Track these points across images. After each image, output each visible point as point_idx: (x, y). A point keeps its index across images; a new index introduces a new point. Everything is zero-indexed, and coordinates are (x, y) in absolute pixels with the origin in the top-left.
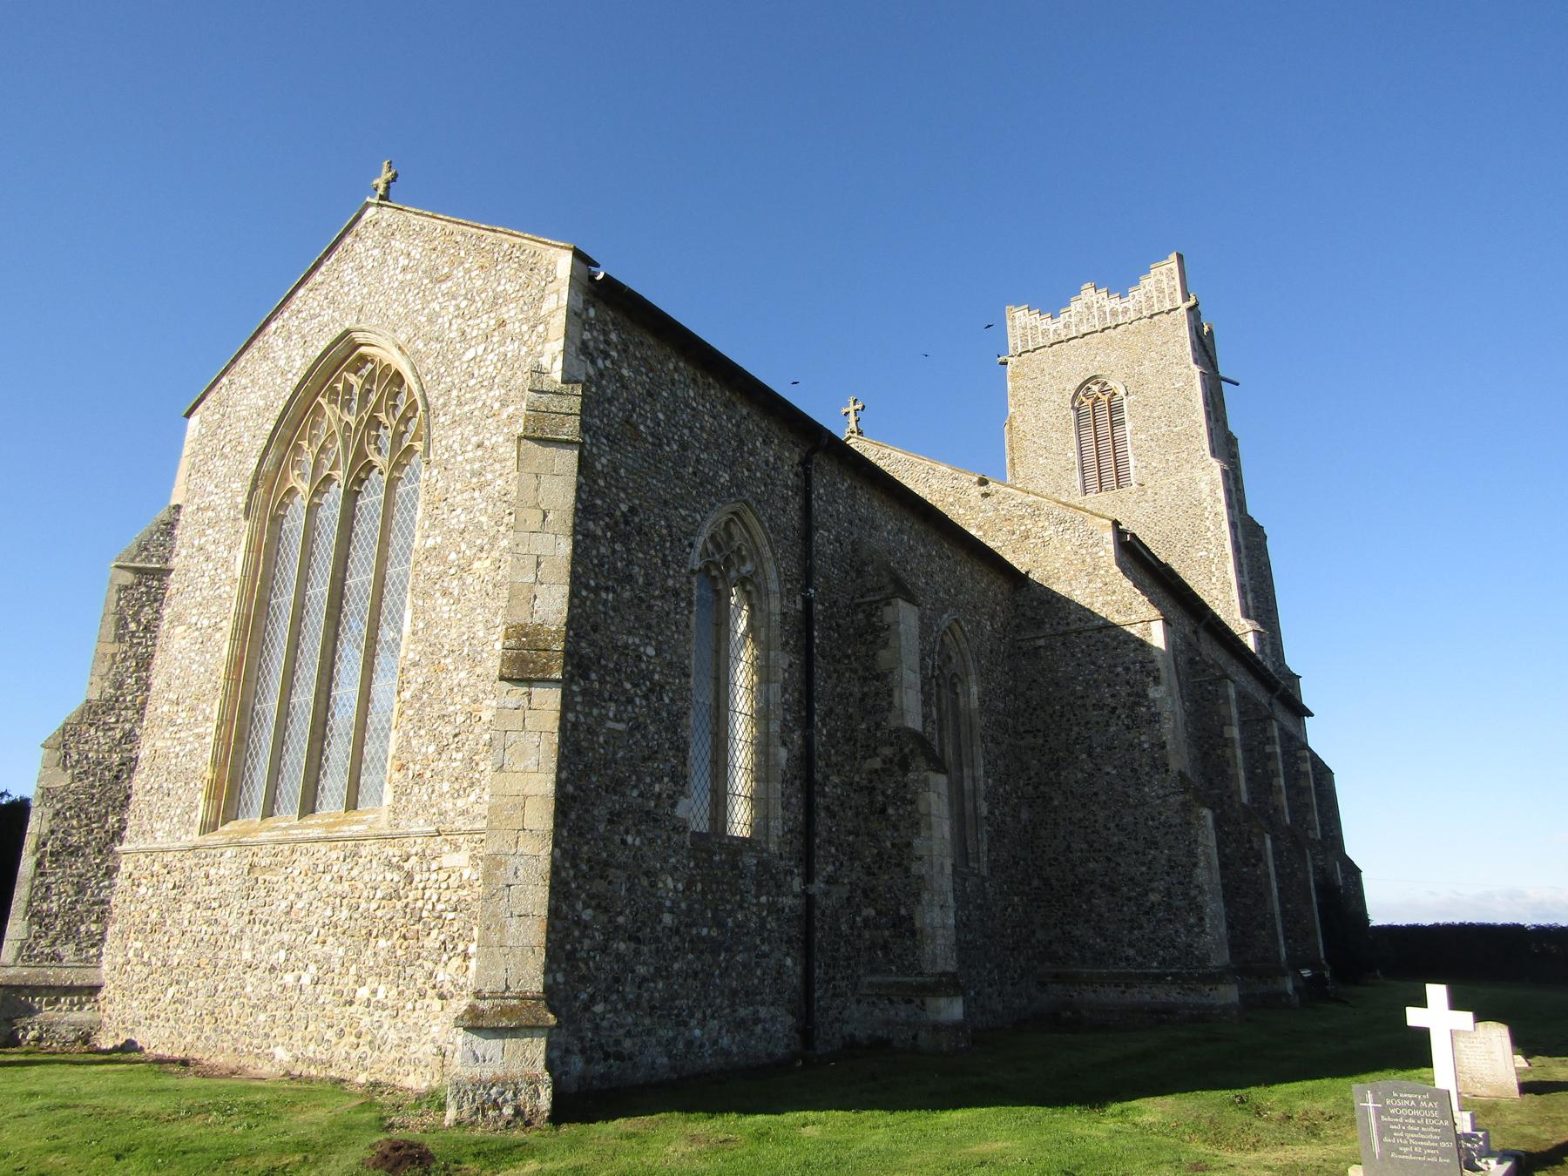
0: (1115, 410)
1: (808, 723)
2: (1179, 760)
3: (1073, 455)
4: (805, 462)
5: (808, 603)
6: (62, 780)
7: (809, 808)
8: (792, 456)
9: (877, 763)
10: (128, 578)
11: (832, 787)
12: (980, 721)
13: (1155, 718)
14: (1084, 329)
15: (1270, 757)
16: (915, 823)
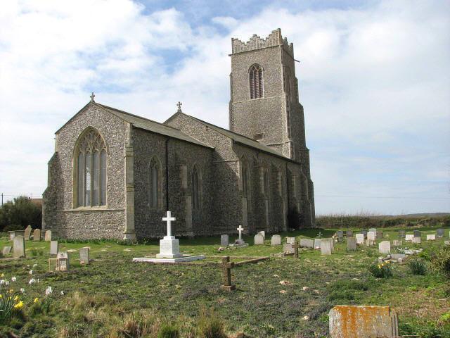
0: (260, 74)
1: (167, 189)
2: (241, 189)
3: (248, 87)
4: (166, 142)
5: (167, 167)
6: (47, 200)
7: (167, 203)
8: (164, 142)
9: (179, 194)
10: (51, 166)
11: (171, 199)
12: (202, 183)
13: (237, 180)
14: (253, 49)
15: (278, 180)
16: (186, 204)
